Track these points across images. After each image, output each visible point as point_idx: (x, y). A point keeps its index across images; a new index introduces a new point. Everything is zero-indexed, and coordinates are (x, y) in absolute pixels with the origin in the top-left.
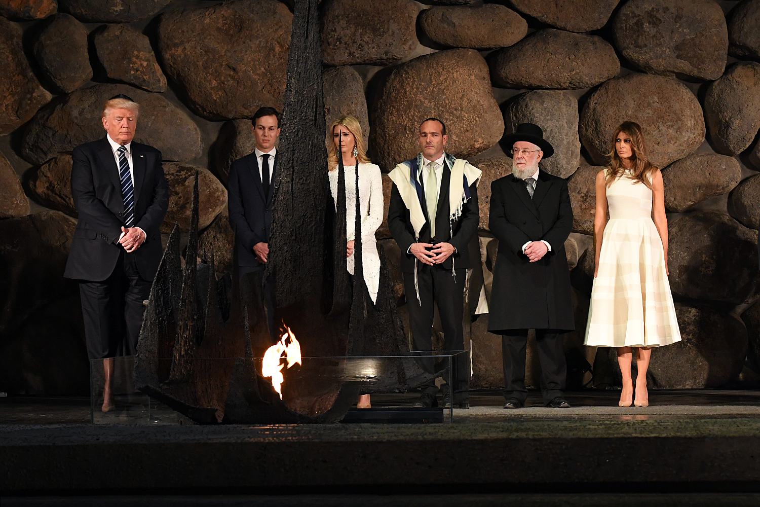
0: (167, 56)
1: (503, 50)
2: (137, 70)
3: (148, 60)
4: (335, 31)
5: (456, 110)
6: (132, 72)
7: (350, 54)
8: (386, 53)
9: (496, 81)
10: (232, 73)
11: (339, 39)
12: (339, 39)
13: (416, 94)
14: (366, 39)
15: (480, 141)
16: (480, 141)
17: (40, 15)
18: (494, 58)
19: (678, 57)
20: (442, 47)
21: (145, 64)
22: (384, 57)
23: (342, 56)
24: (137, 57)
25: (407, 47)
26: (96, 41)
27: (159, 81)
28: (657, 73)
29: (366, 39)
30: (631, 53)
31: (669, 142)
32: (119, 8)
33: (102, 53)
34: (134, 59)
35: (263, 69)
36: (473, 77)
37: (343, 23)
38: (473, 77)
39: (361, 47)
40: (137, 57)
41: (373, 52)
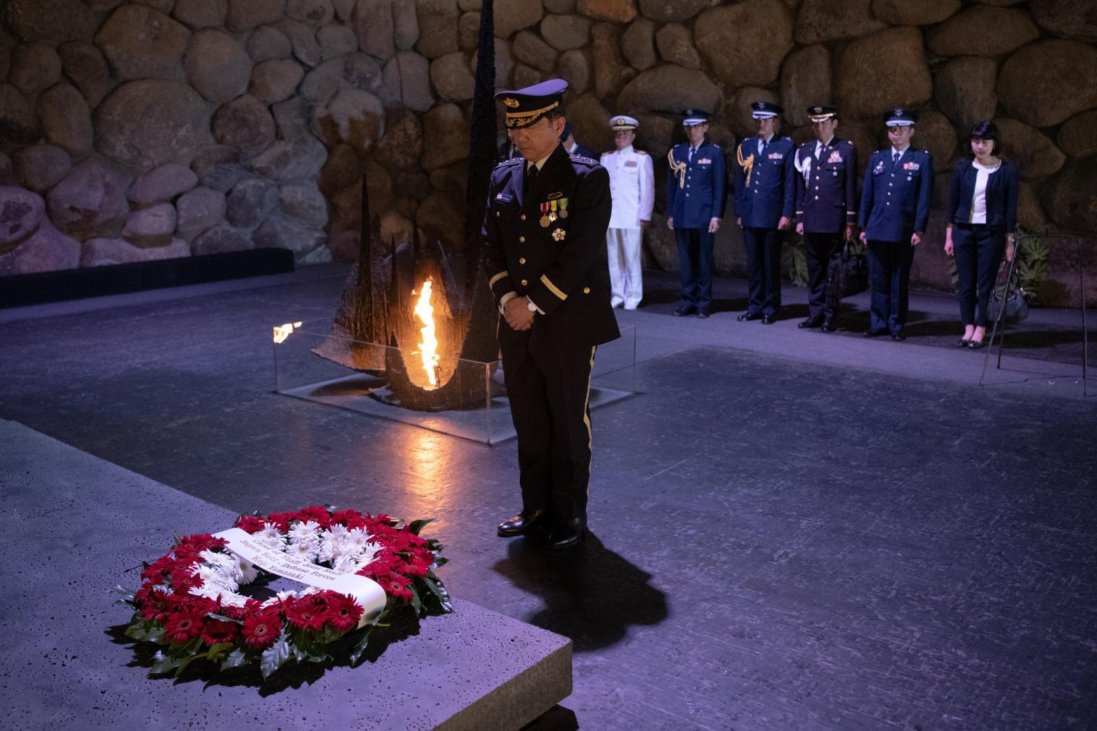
0: (698, 43)
1: (936, 25)
2: (680, 54)
3: (688, 47)
4: (807, 18)
5: (891, 75)
6: (677, 56)
7: (818, 35)
8: (844, 33)
9: (927, 50)
10: (737, 53)
11: (810, 24)
12: (810, 24)
13: (862, 64)
14: (829, 22)
15: (910, 99)
16: (910, 99)
17: (627, 20)
18: (927, 32)
19: (1087, 23)
20: (892, 26)
21: (685, 49)
22: (843, 36)
23: (811, 37)
24: (681, 45)
25: (861, 25)
26: (657, 35)
27: (695, 61)
28: (554, 14)
29: (829, 22)
30: (1045, 22)
31: (1070, 98)
32: (670, 11)
33: (659, 43)
34: (679, 47)
35: (757, 50)
36: (907, 49)
37: (814, 12)
38: (907, 49)
39: (825, 29)
40: (681, 45)
41: (835, 33)
